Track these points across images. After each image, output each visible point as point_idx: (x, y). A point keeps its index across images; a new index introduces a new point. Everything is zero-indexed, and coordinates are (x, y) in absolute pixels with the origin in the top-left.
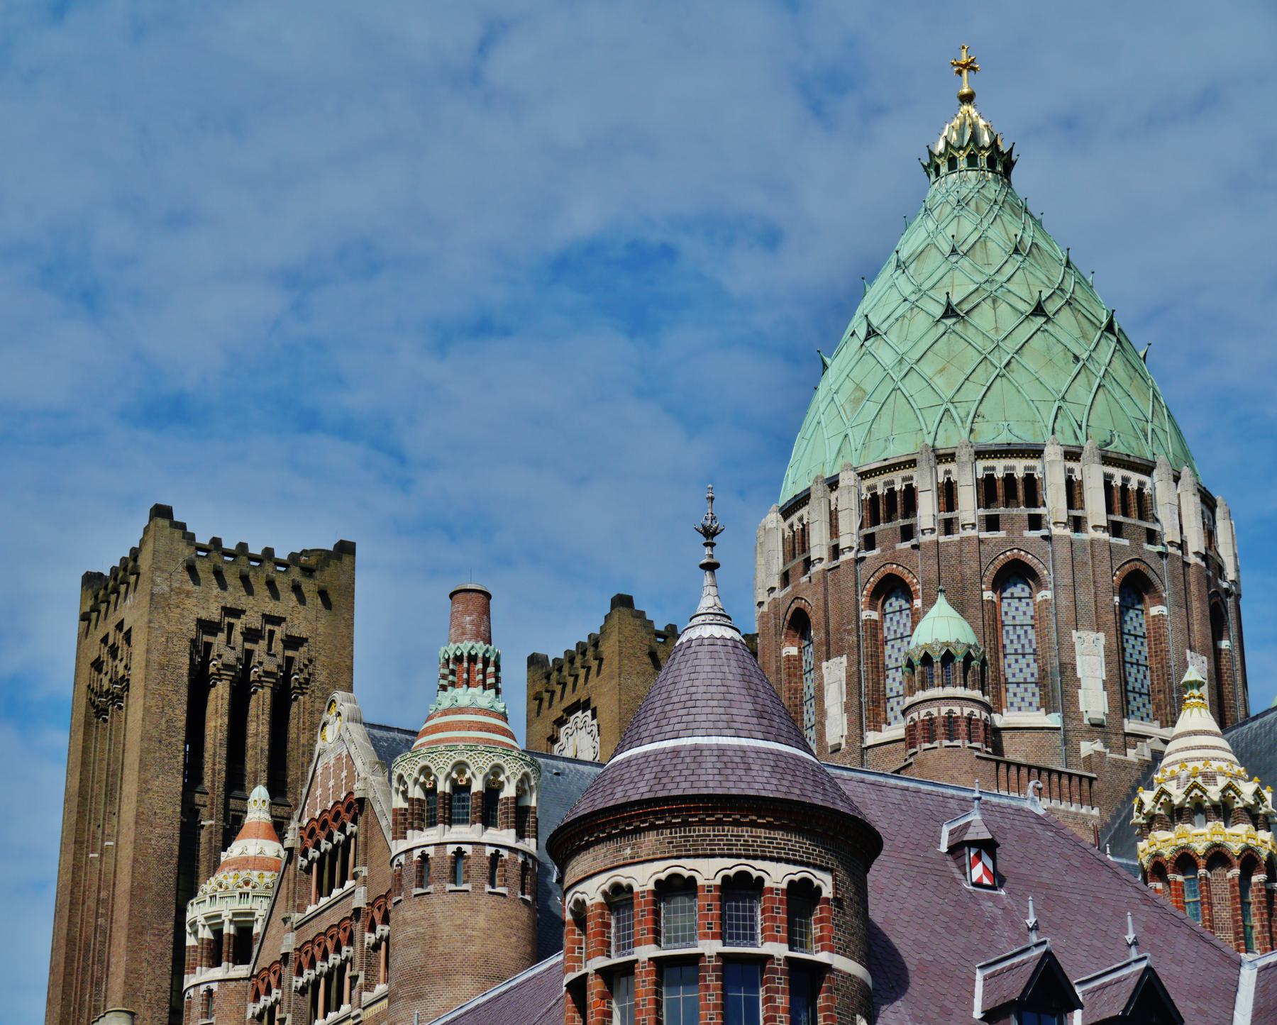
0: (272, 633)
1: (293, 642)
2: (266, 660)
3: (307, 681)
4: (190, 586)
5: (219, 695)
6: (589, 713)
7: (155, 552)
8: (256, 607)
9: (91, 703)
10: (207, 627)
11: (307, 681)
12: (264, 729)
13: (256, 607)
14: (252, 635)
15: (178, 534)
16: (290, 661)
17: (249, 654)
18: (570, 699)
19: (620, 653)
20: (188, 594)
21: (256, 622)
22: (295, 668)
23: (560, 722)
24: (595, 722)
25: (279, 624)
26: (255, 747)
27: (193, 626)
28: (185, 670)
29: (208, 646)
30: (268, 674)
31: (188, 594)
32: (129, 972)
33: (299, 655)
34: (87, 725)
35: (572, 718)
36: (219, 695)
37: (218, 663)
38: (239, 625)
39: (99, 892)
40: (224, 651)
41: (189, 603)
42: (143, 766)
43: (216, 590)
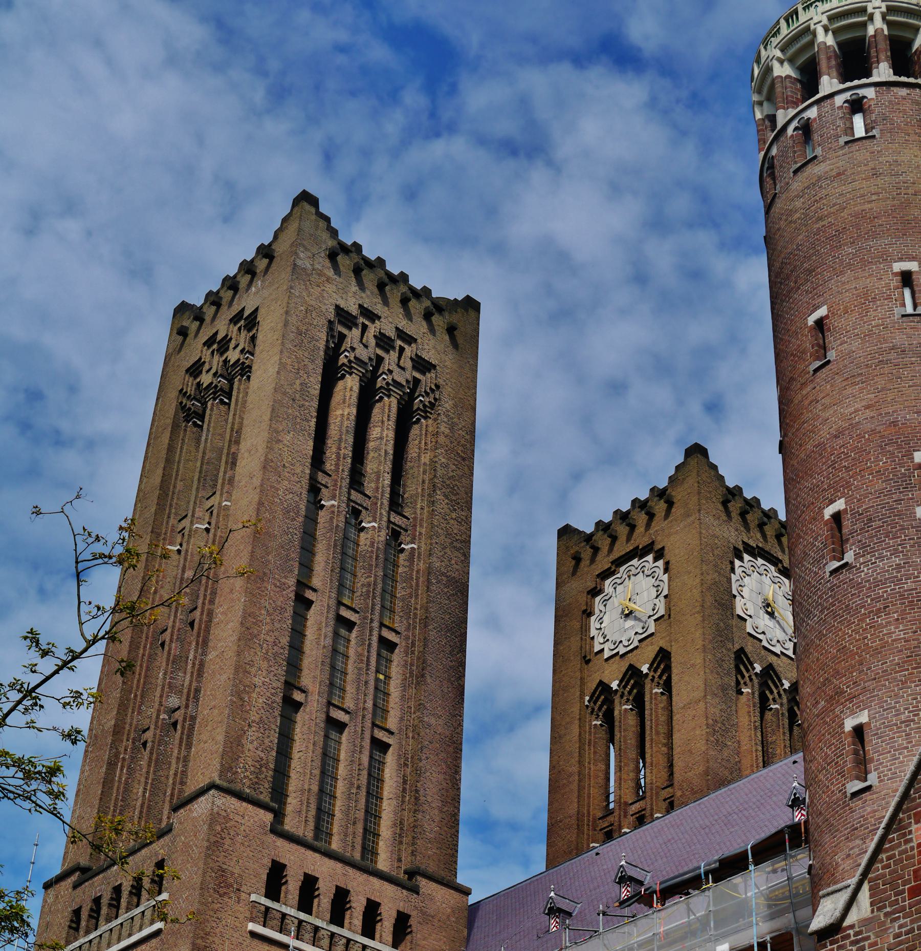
0: (402, 350)
1: (422, 365)
2: (396, 369)
3: (432, 405)
4: (331, 273)
5: (348, 387)
6: (650, 558)
7: (300, 230)
8: (391, 320)
9: (182, 407)
10: (344, 317)
11: (432, 405)
12: (390, 434)
13: (391, 320)
14: (384, 342)
15: (322, 224)
16: (417, 381)
17: (380, 360)
18: (622, 548)
19: (699, 493)
20: (328, 280)
21: (391, 333)
22: (421, 389)
23: (606, 574)
24: (660, 563)
25: (410, 344)
26: (377, 449)
27: (332, 309)
28: (322, 345)
29: (342, 337)
30: (396, 384)
31: (328, 280)
32: (246, 615)
33: (427, 380)
34: (175, 426)
35: (622, 569)
36: (348, 387)
37: (352, 356)
38: (372, 329)
39: (183, 571)
40: (359, 345)
41: (330, 288)
42: (274, 415)
43: (354, 288)
